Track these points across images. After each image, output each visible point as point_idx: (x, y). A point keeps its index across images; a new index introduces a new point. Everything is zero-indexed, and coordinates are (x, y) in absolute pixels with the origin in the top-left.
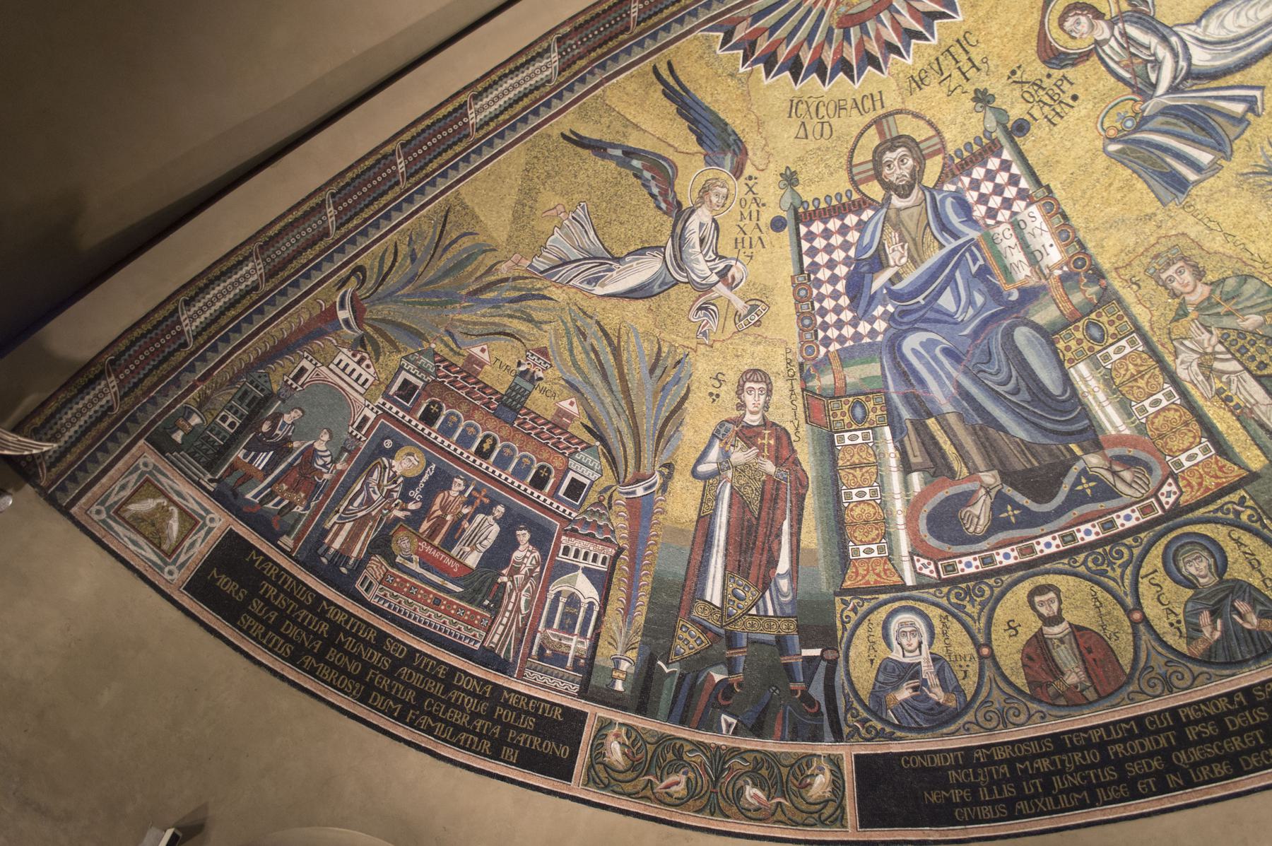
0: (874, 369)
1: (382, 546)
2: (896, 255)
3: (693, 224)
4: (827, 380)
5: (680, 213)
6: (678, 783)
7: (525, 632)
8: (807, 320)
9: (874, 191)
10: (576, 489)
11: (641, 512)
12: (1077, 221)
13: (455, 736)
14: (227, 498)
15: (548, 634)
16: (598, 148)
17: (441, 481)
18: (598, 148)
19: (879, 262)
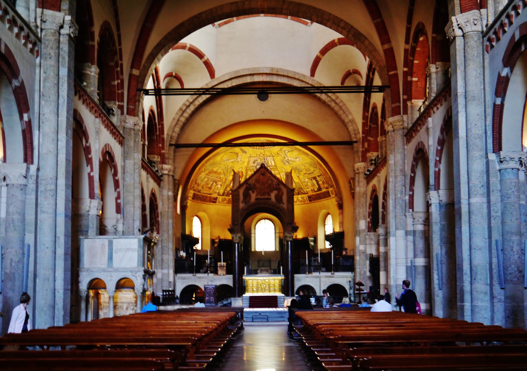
0: (253, 168)
1: (203, 188)
2: (259, 160)
3: (239, 157)
4: (248, 168)
5: (238, 156)
6: (225, 202)
7: (214, 191)
8: (248, 164)
9: (258, 156)
10: (220, 178)
11: (226, 179)
12: (276, 163)
13: (207, 201)
14: (195, 190)
15: (215, 191)
16: (232, 152)
17: (208, 180)
18: (232, 152)
19: (257, 160)
